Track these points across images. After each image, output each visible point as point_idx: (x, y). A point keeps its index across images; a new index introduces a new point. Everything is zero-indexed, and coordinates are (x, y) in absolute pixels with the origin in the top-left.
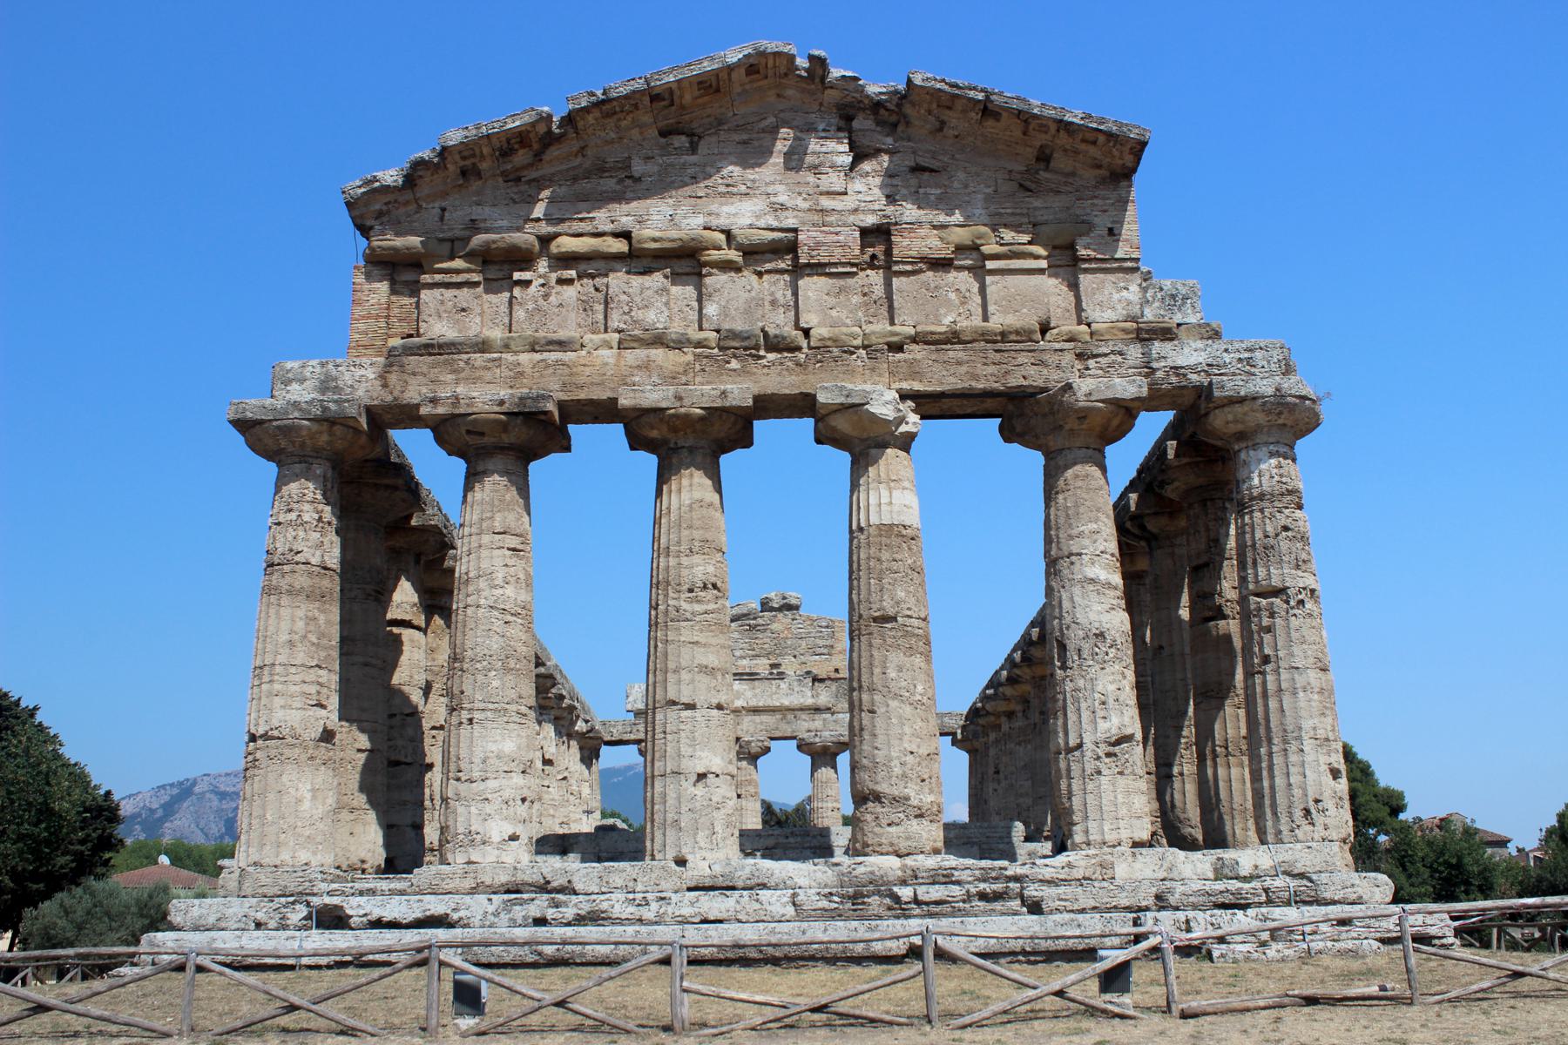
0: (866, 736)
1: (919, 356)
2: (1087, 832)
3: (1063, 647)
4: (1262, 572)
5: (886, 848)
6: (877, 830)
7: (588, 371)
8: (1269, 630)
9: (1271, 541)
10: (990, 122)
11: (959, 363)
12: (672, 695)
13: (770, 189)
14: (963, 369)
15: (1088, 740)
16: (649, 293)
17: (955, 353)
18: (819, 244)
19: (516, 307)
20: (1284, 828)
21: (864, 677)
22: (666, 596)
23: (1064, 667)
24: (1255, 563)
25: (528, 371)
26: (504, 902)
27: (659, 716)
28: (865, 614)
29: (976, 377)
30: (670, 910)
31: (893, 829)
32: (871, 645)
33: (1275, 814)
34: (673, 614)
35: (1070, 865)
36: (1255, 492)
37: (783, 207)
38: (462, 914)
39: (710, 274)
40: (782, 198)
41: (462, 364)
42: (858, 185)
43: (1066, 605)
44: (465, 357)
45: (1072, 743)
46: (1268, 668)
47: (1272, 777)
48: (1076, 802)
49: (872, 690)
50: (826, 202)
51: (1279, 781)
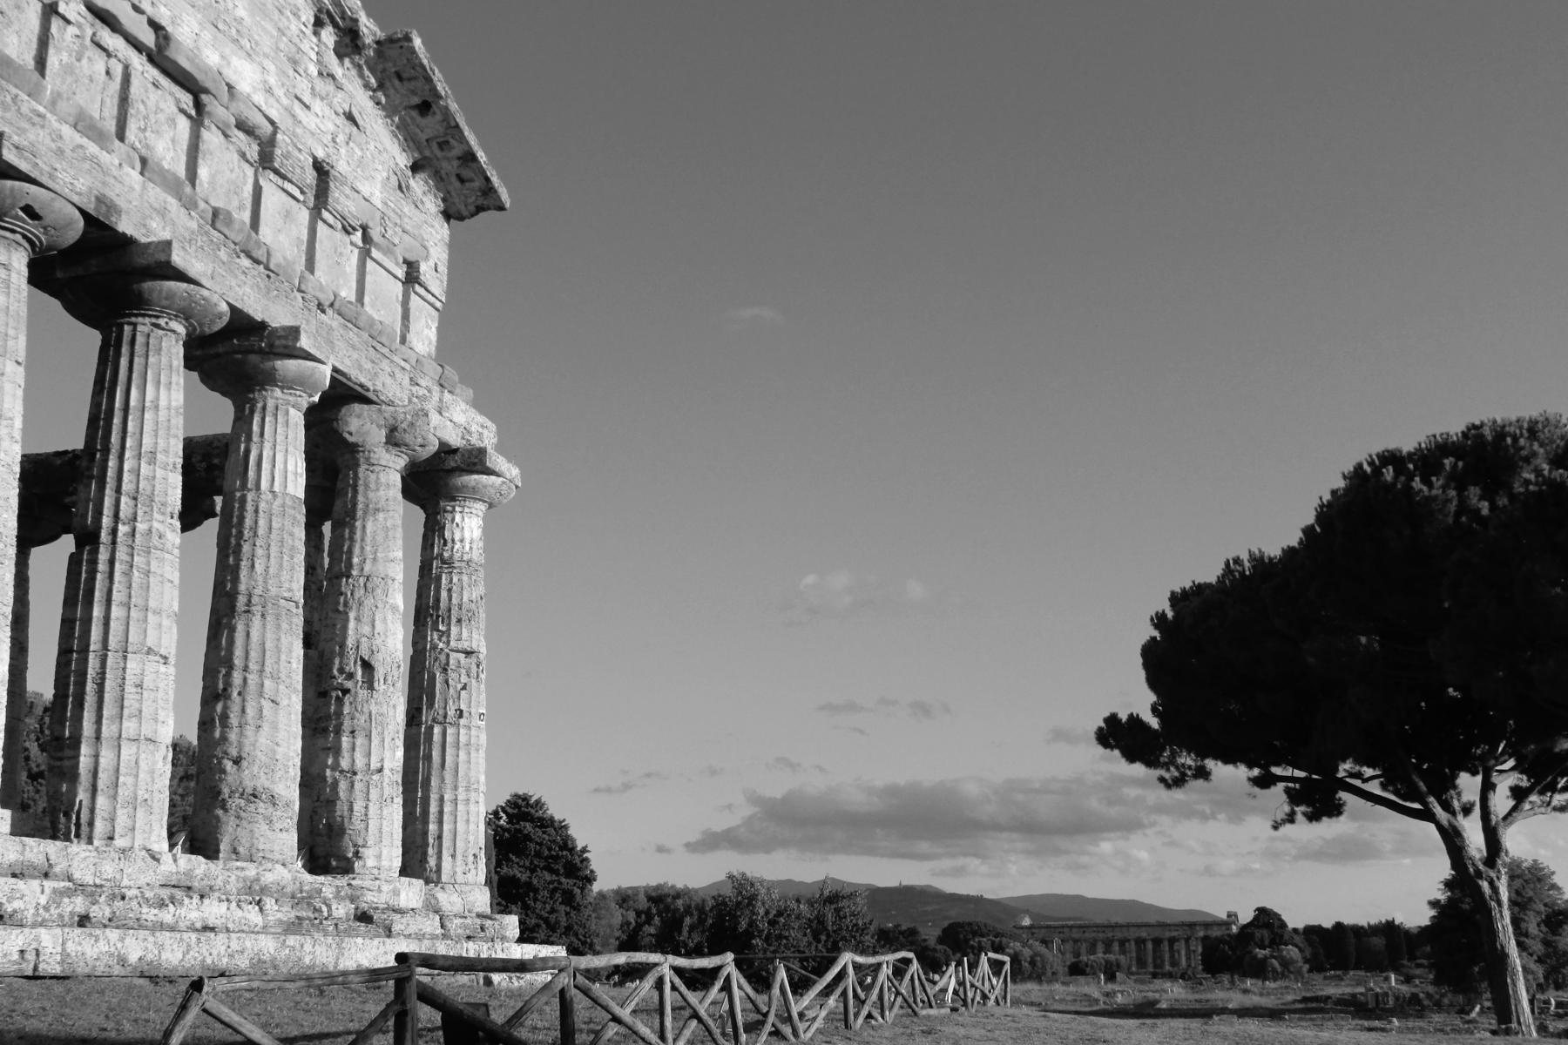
0: (266, 727)
1: (335, 324)
2: (379, 857)
3: (367, 666)
4: (465, 634)
5: (277, 856)
6: (269, 833)
7: (118, 188)
8: (464, 688)
9: (473, 606)
10: (414, 113)
11: (353, 347)
12: (150, 642)
13: (266, 63)
14: (355, 356)
15: (387, 765)
16: (162, 117)
17: (352, 334)
18: (287, 156)
19: (51, 51)
20: (459, 870)
21: (268, 662)
22: (149, 514)
23: (371, 687)
24: (459, 621)
25: (68, 153)
26: (55, 891)
27: (133, 665)
28: (273, 591)
29: (360, 368)
30: (182, 911)
31: (280, 835)
32: (278, 627)
33: (453, 856)
34: (155, 538)
35: (379, 891)
36: (466, 558)
37: (269, 91)
38: (17, 904)
39: (209, 129)
40: (272, 80)
41: (8, 99)
42: (317, 106)
43: (379, 626)
44: (15, 91)
45: (374, 765)
46: (462, 721)
47: (440, 822)
48: (373, 824)
49: (276, 678)
50: (298, 108)
51: (461, 827)
